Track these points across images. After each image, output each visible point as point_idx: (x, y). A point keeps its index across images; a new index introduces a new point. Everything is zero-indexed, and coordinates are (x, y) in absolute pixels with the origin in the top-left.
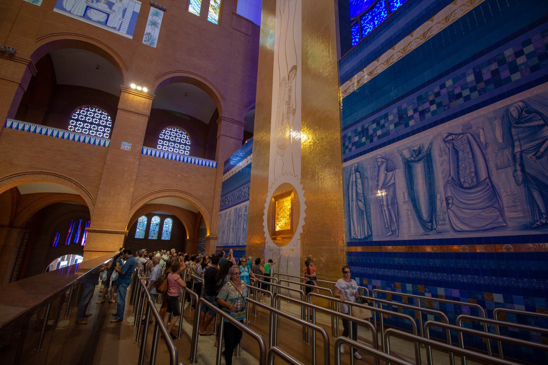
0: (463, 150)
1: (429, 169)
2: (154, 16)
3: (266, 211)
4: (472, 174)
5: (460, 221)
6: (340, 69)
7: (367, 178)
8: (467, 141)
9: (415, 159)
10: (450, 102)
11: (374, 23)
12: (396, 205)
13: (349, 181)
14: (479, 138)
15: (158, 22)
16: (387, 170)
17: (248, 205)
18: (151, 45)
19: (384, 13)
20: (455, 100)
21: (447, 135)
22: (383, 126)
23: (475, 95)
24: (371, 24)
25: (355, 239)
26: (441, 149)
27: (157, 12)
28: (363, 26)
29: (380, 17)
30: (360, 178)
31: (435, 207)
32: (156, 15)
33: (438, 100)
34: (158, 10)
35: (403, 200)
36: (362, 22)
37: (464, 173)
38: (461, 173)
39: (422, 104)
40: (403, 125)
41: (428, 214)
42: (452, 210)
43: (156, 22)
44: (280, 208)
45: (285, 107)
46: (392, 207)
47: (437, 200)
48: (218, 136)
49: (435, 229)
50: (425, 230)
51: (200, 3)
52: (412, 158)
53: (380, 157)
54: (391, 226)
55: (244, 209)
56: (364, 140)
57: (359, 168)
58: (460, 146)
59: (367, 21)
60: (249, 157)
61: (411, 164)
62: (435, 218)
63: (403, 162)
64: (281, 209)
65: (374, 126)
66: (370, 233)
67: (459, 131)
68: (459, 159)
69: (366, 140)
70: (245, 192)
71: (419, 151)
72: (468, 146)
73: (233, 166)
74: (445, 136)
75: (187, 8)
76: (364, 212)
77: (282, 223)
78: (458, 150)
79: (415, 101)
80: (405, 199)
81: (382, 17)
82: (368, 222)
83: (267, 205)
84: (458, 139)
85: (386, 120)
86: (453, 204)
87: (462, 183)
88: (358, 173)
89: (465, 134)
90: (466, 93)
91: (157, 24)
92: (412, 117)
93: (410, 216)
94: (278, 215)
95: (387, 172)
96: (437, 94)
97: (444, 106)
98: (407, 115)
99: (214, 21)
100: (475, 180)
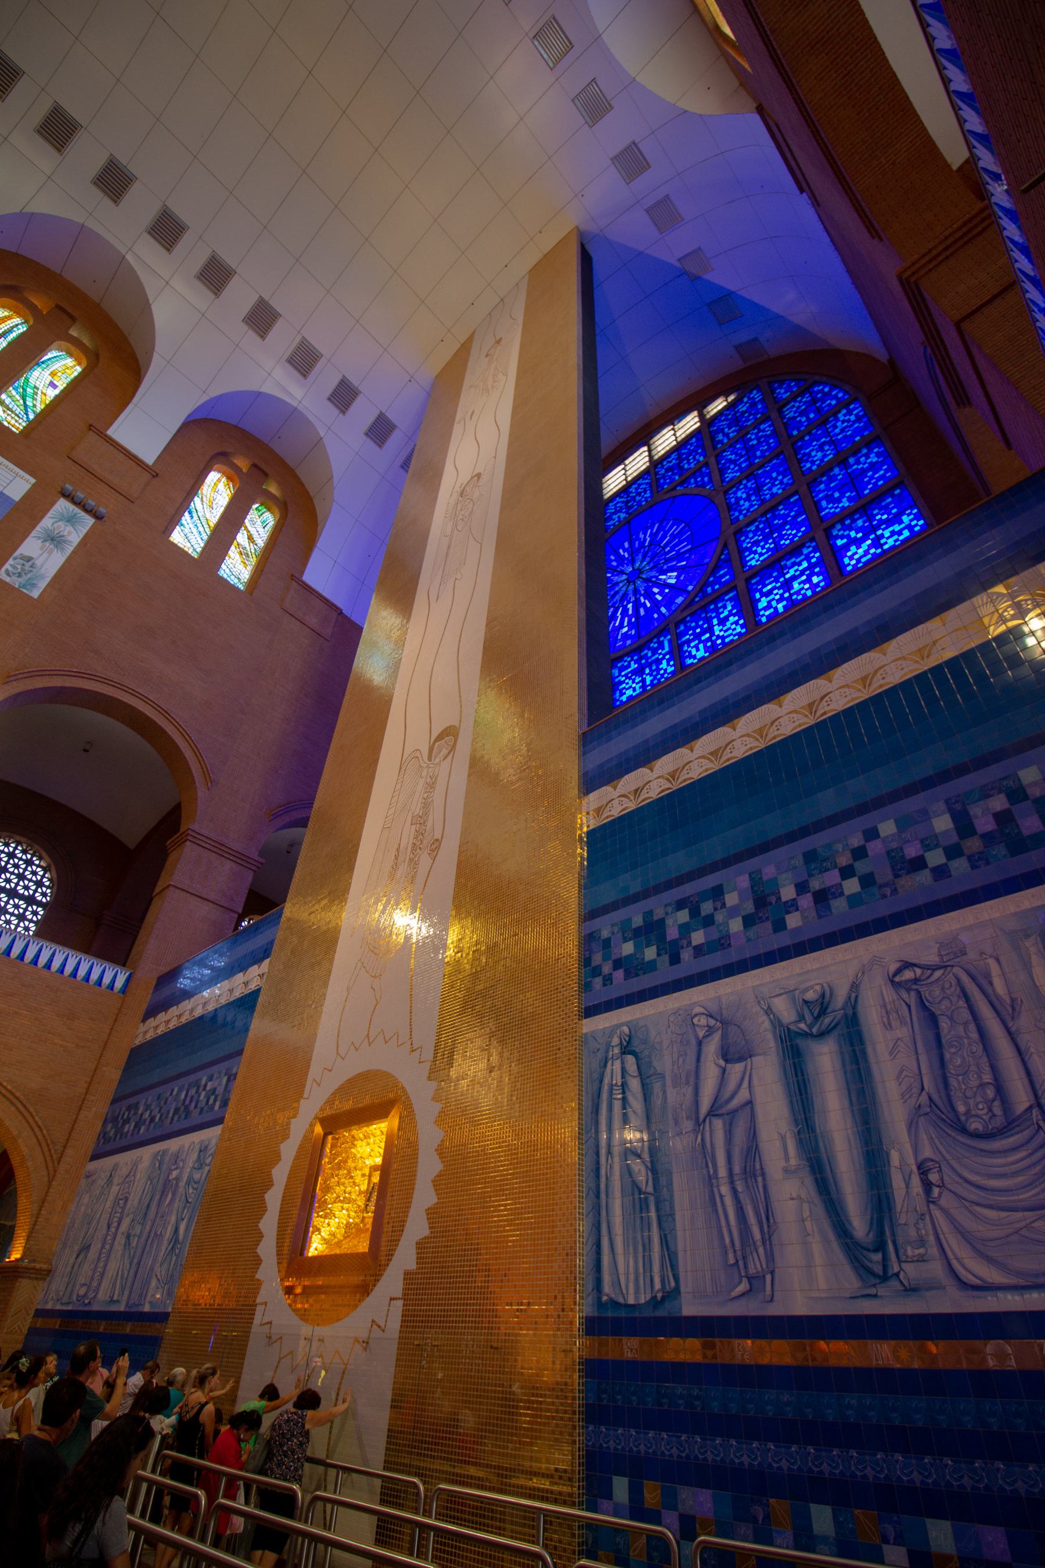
0: (949, 1013)
1: (858, 1064)
2: (61, 520)
3: (280, 1174)
4: (989, 1092)
5: (974, 1247)
6: (584, 754)
7: (662, 1076)
8: (958, 988)
9: (810, 1026)
10: (897, 876)
11: (643, 681)
12: (760, 1179)
13: (601, 1081)
14: (991, 983)
15: (70, 538)
16: (728, 1055)
17: (214, 1142)
18: (24, 586)
19: (668, 664)
20: (908, 873)
21: (898, 965)
22: (708, 921)
23: (960, 866)
24: (637, 681)
25: (615, 1304)
26: (884, 1006)
27: (75, 515)
28: (617, 680)
29: (658, 670)
30: (636, 1074)
31: (886, 1194)
32: (68, 521)
33: (862, 867)
34: (79, 511)
35: (783, 1163)
36: (616, 672)
37: (964, 1087)
38: (956, 1085)
39: (821, 872)
40: (769, 925)
41: (868, 1217)
42: (942, 1209)
43: (63, 536)
44: (339, 1163)
45: (408, 833)
46: (748, 1187)
47: (893, 1170)
48: (158, 889)
49: (897, 1275)
50: (862, 1280)
51: (207, 530)
52: (802, 1026)
53: (702, 1010)
54: (744, 1258)
55: (194, 1156)
56: (650, 953)
57: (635, 1042)
58: (940, 1002)
59: (626, 672)
60: (254, 971)
61: (801, 1042)
62: (893, 1235)
63: (774, 1033)
64: (339, 1166)
65: (683, 916)
66: (673, 1284)
67: (931, 957)
68: (944, 1040)
69: (659, 955)
70: (214, 1090)
71: (822, 1006)
72: (962, 1003)
73: (187, 995)
74: (893, 967)
75: (169, 530)
76: (652, 1199)
77: (334, 1222)
78: (938, 1012)
79: (799, 861)
80: (787, 1158)
81: (662, 672)
82: (665, 1241)
83: (289, 1150)
84: (929, 981)
85: (719, 904)
86: (942, 1186)
87: (963, 1118)
88: (630, 1059)
89: (949, 969)
90: (935, 858)
91: (65, 542)
92: (792, 906)
93: (808, 1224)
94: (327, 1189)
95: (727, 1061)
96: (859, 853)
97: (881, 887)
98: (780, 898)
99: (236, 581)
100: (997, 1110)
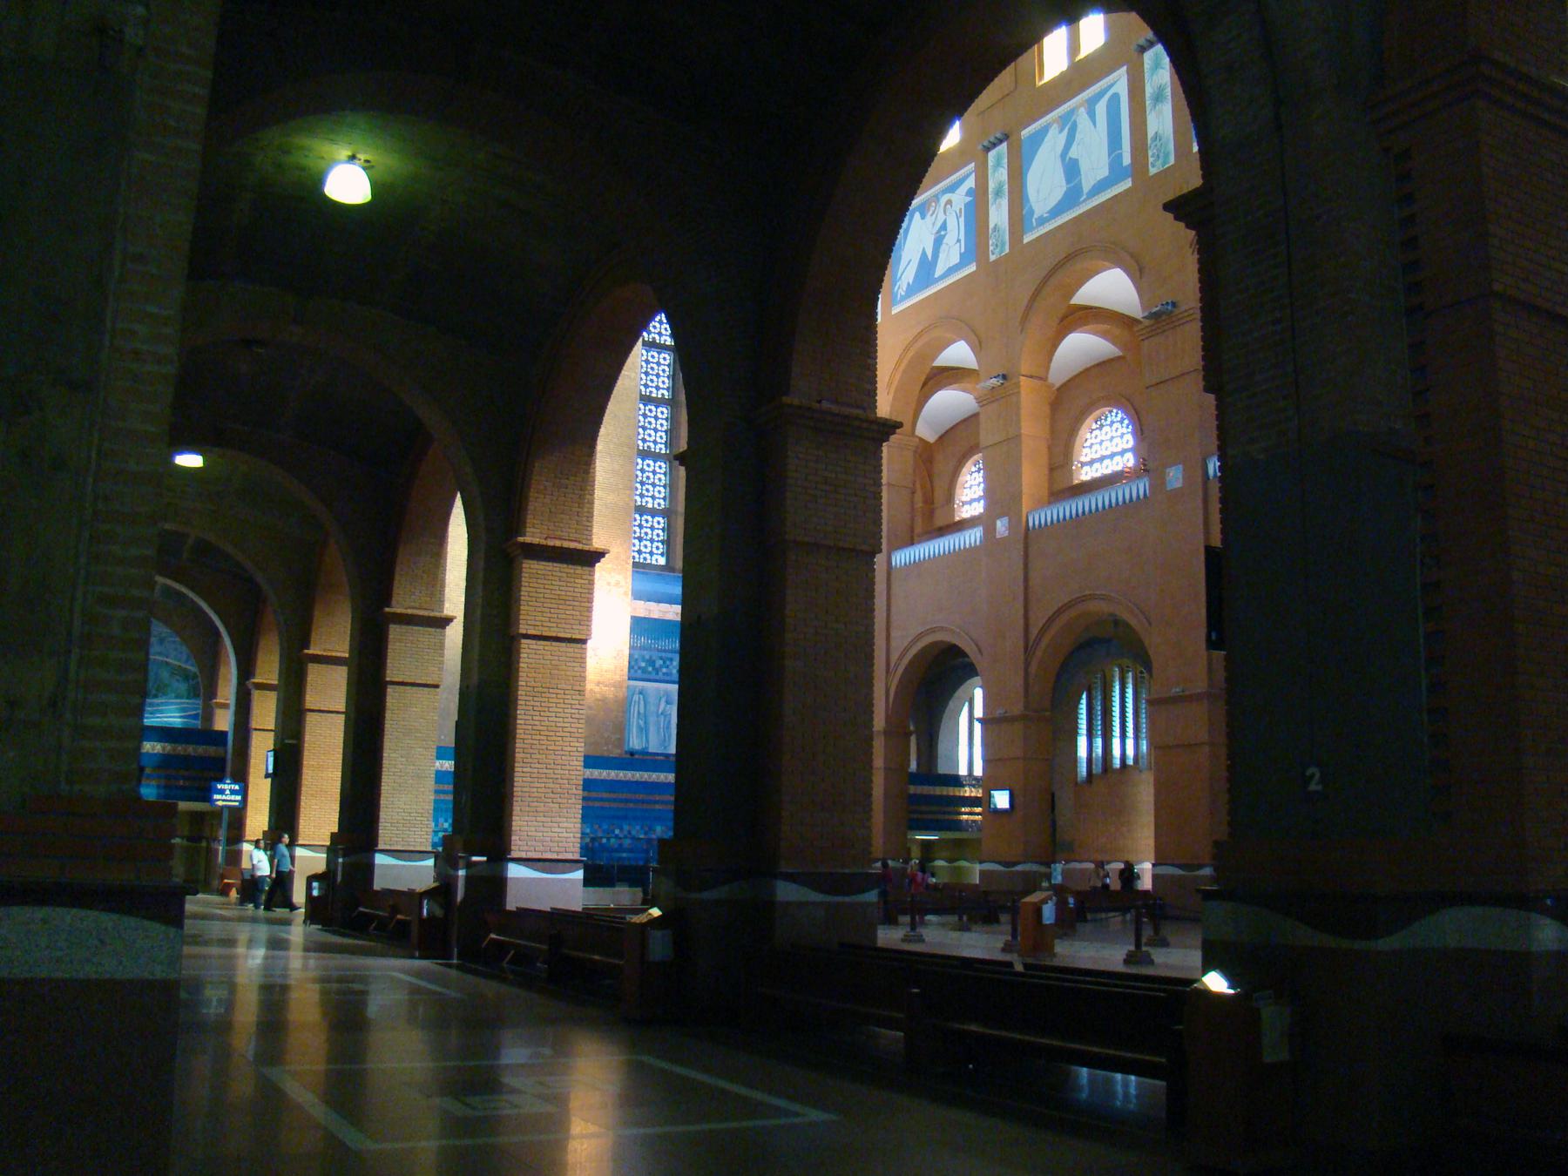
88: (641, 696)
